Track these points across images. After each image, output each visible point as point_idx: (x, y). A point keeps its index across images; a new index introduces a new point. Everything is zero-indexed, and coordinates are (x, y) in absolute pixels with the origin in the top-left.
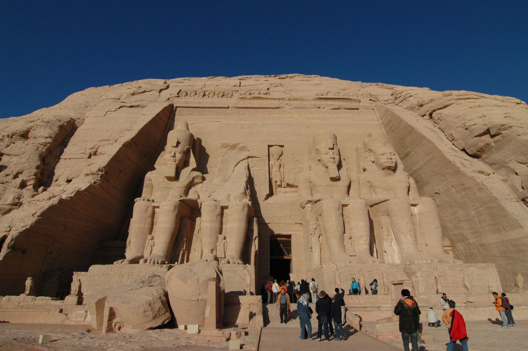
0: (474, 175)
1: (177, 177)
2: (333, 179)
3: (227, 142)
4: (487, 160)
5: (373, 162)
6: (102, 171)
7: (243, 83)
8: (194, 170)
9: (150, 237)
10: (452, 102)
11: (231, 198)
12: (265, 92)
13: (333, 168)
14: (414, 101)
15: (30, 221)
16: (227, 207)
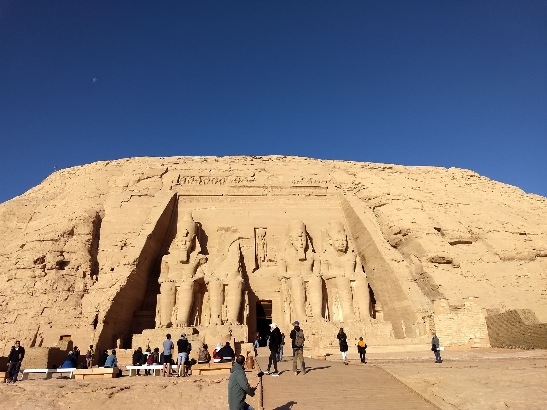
0: (389, 262)
1: (188, 261)
2: (301, 260)
3: (223, 226)
4: (401, 251)
5: (331, 245)
6: (136, 261)
7: (233, 167)
8: (200, 253)
9: (174, 308)
10: (387, 202)
11: (229, 276)
12: (252, 179)
13: (301, 251)
14: (365, 193)
15: (109, 304)
16: (227, 285)
